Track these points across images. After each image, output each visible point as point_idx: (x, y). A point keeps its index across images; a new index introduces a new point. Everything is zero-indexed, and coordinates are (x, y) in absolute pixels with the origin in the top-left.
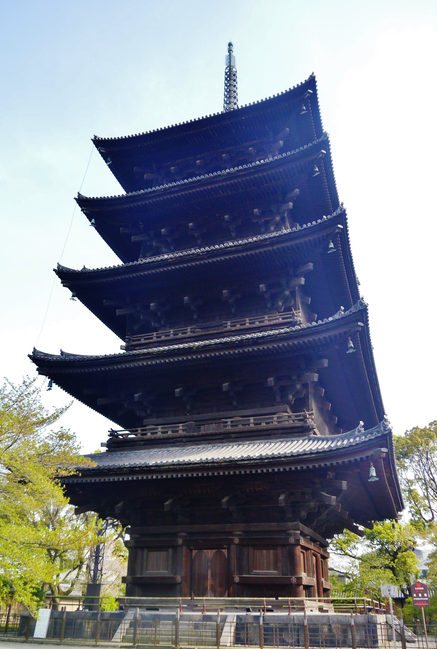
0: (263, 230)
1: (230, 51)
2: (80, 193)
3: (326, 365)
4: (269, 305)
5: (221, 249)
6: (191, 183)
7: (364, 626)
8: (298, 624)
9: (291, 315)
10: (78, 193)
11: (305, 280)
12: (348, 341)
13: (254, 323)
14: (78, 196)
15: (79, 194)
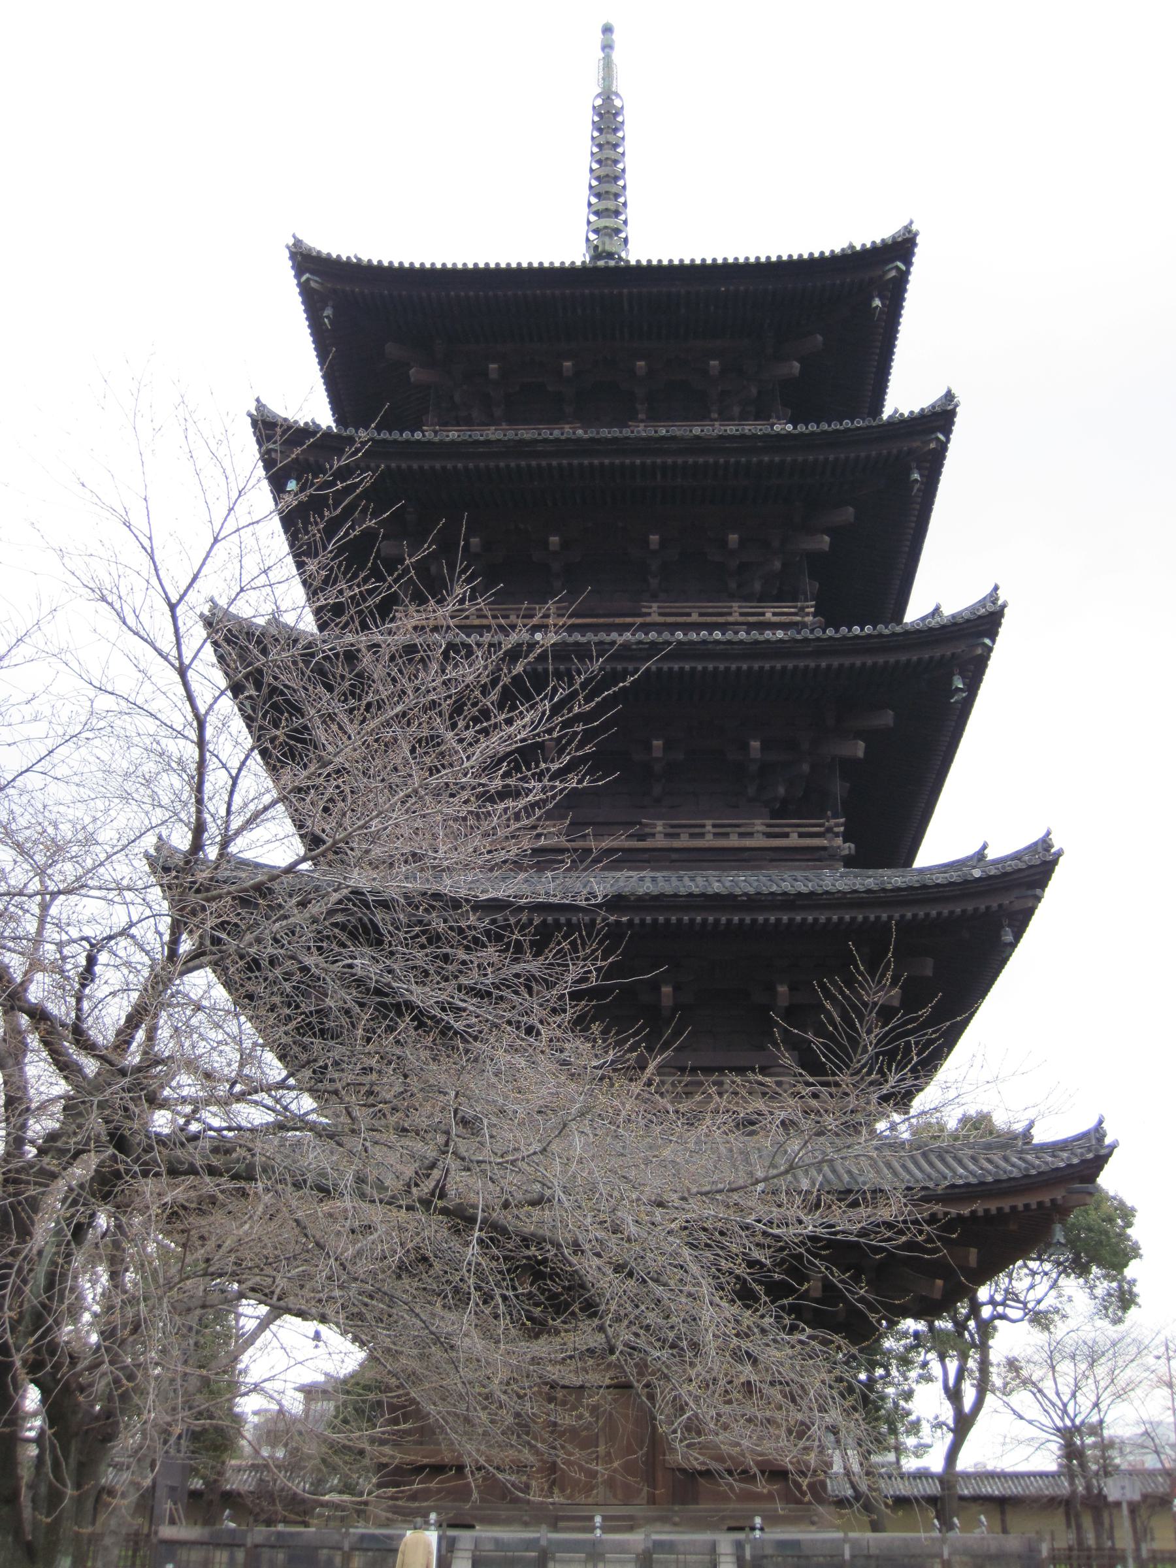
0: (733, 585)
1: (607, 47)
2: (264, 401)
3: (929, 972)
4: (751, 791)
5: (691, 643)
6: (592, 440)
7: (1019, 1557)
8: (877, 1557)
9: (822, 829)
10: (258, 400)
11: (866, 748)
12: (1001, 927)
13: (726, 835)
14: (257, 409)
15: (260, 406)
